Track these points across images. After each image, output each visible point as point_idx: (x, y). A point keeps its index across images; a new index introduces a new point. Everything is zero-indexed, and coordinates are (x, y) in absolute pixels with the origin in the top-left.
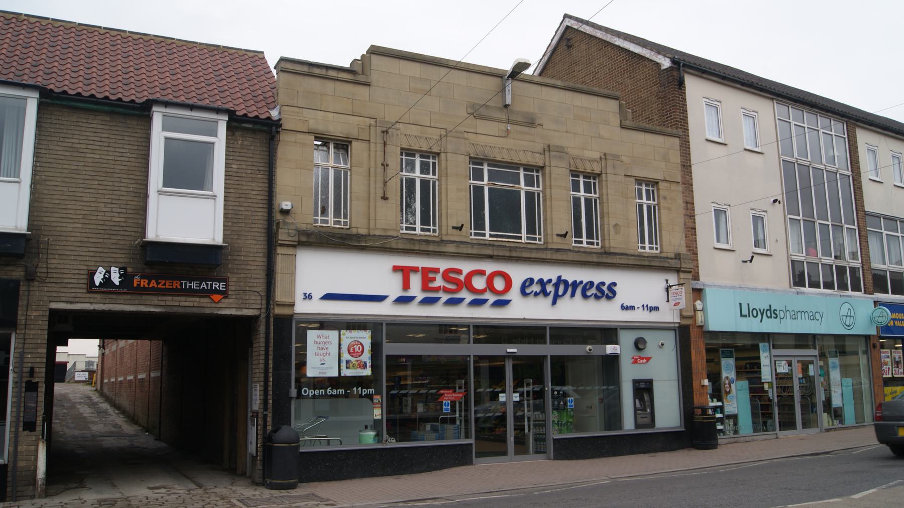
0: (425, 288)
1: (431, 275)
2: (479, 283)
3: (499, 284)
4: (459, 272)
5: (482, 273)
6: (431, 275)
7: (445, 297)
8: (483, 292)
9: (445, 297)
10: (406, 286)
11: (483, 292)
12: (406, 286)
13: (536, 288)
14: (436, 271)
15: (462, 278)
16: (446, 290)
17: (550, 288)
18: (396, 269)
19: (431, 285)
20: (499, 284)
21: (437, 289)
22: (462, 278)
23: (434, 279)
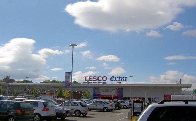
1: (91, 78)
2: (100, 79)
3: (105, 79)
6: (91, 78)
7: (93, 82)
8: (101, 80)
10: (86, 80)
11: (101, 80)
13: (115, 79)
15: (97, 78)
17: (118, 79)
18: (84, 77)
19: (90, 79)
20: (105, 79)
21: (92, 80)
22: (97, 78)
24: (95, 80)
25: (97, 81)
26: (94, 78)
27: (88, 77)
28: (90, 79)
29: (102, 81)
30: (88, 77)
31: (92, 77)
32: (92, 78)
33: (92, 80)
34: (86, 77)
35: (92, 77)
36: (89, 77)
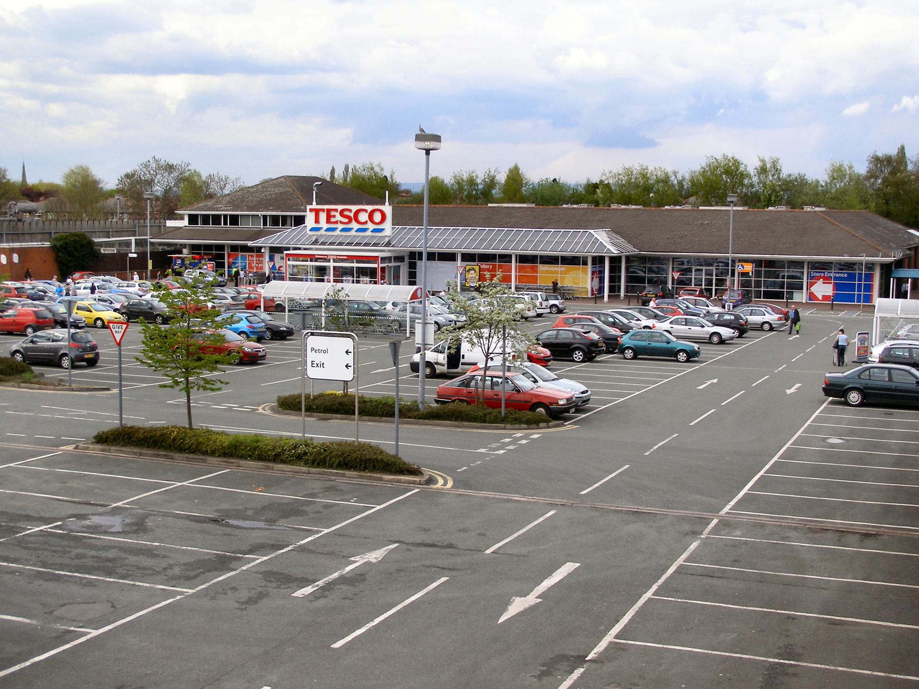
0: (328, 221)
1: (333, 213)
2: (363, 217)
4: (350, 211)
5: (366, 211)
6: (333, 213)
7: (340, 226)
9: (340, 226)
11: (366, 223)
14: (336, 210)
15: (352, 215)
16: (341, 222)
19: (333, 220)
21: (336, 222)
22: (352, 215)
23: (334, 216)
24: (346, 220)
29: (371, 226)
30: (323, 210)
32: (337, 215)
33: (336, 222)
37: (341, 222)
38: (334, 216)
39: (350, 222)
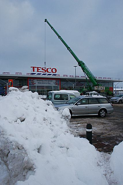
0: (38, 71)
1: (39, 69)
2: (50, 70)
3: (54, 70)
6: (39, 69)
8: (51, 72)
10: (34, 71)
12: (34, 71)
15: (46, 69)
16: (42, 72)
18: (31, 67)
19: (39, 71)
20: (54, 70)
21: (41, 72)
22: (46, 69)
23: (40, 70)
24: (44, 71)
25: (46, 73)
26: (42, 69)
27: (36, 67)
28: (39, 71)
29: (52, 74)
30: (36, 67)
31: (40, 68)
33: (41, 72)
34: (34, 68)
35: (40, 68)
36: (38, 68)
37: (42, 72)
38: (40, 70)
39: (45, 72)
